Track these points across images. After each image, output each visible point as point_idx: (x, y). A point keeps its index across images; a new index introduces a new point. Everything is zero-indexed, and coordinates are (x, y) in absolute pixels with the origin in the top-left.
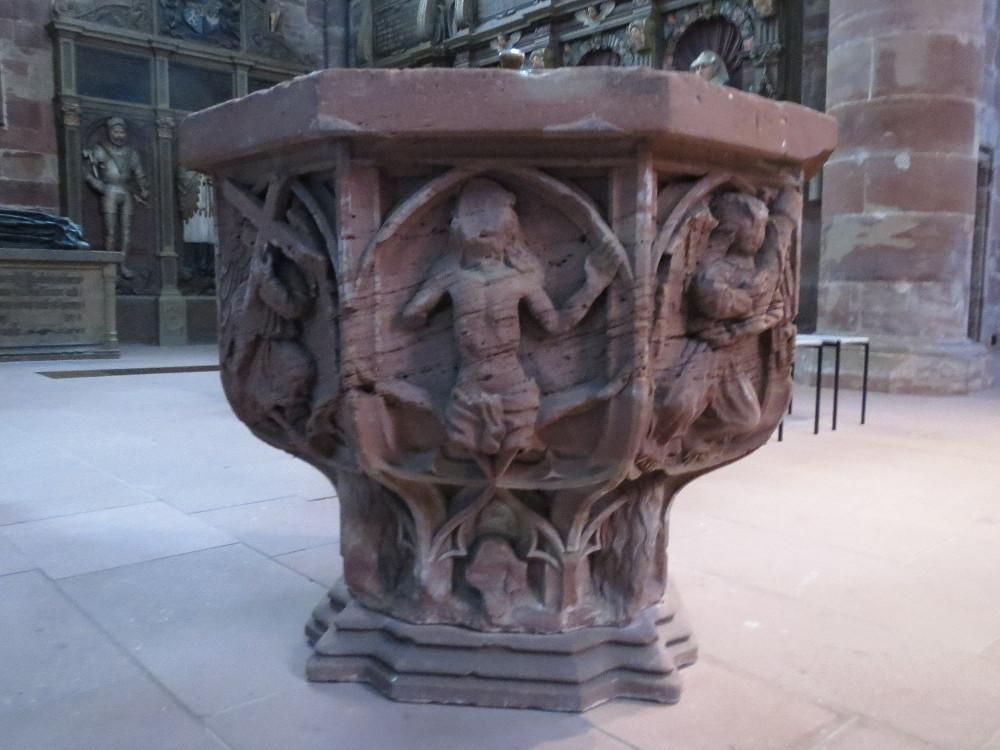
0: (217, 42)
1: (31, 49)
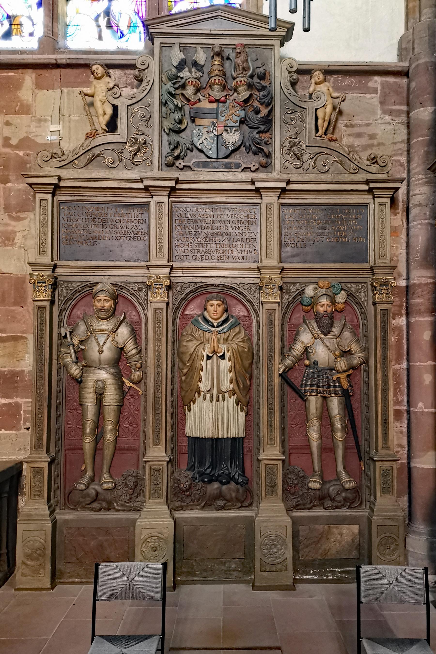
0: (238, 166)
1: (22, 215)
